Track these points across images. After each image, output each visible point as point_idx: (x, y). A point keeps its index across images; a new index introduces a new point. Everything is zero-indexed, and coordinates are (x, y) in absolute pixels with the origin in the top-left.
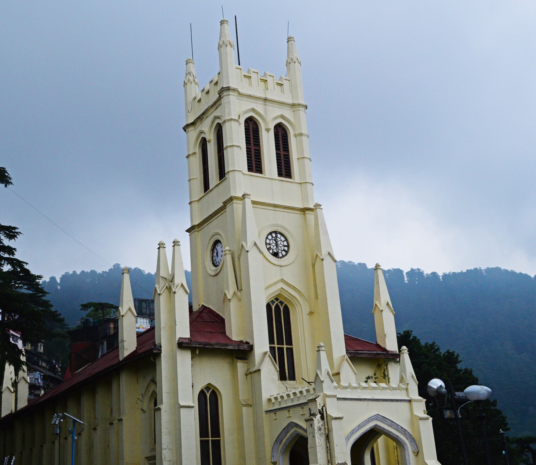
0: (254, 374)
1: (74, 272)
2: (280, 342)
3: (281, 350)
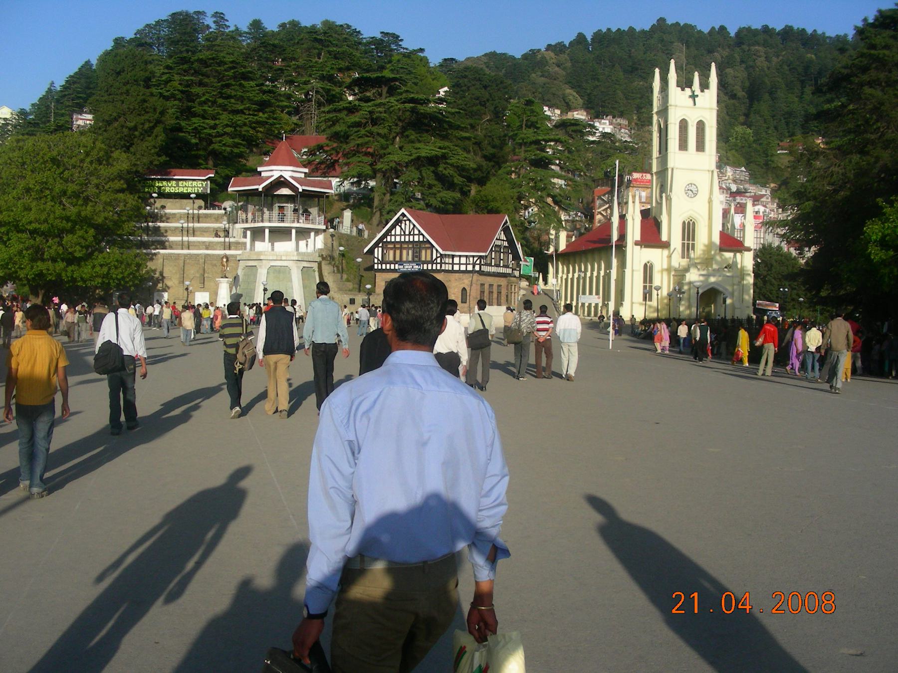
0: (670, 257)
1: (609, 29)
2: (688, 240)
3: (688, 244)
